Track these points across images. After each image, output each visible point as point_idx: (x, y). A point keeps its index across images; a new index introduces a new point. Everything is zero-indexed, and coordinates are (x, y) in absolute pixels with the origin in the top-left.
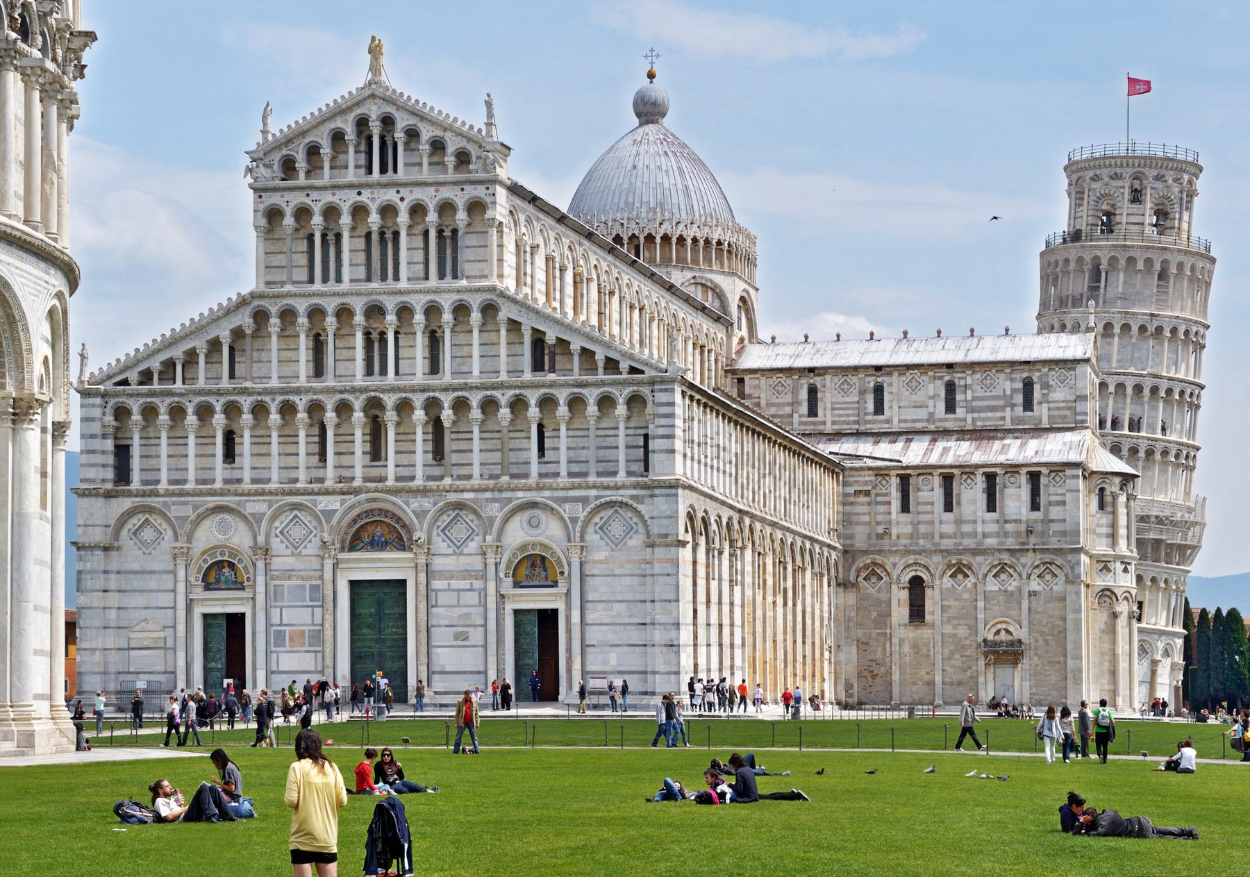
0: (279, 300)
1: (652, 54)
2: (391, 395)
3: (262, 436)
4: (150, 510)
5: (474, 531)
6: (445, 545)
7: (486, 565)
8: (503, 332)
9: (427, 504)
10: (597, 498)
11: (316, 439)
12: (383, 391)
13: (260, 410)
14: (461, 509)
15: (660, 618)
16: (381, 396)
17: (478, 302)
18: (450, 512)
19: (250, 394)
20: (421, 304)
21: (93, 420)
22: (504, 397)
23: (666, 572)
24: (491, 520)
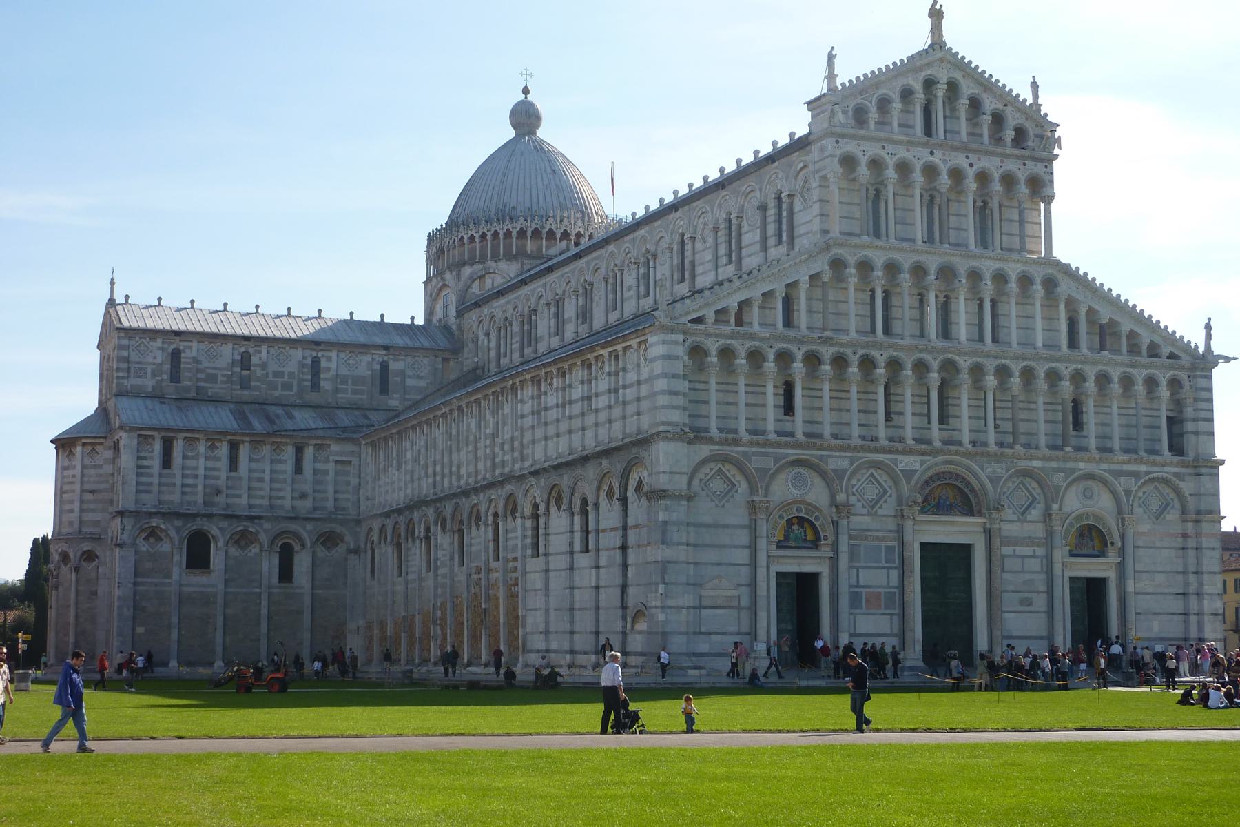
1: (526, 73)
2: (966, 358)
4: (726, 459)
5: (1034, 499)
7: (1050, 534)
8: (1062, 307)
9: (999, 470)
10: (1147, 473)
11: (893, 398)
12: (960, 354)
13: (840, 362)
15: (1207, 589)
17: (1042, 274)
18: (1015, 479)
19: (831, 345)
21: (676, 358)
22: (1066, 370)
23: (1212, 546)
24: (1058, 489)
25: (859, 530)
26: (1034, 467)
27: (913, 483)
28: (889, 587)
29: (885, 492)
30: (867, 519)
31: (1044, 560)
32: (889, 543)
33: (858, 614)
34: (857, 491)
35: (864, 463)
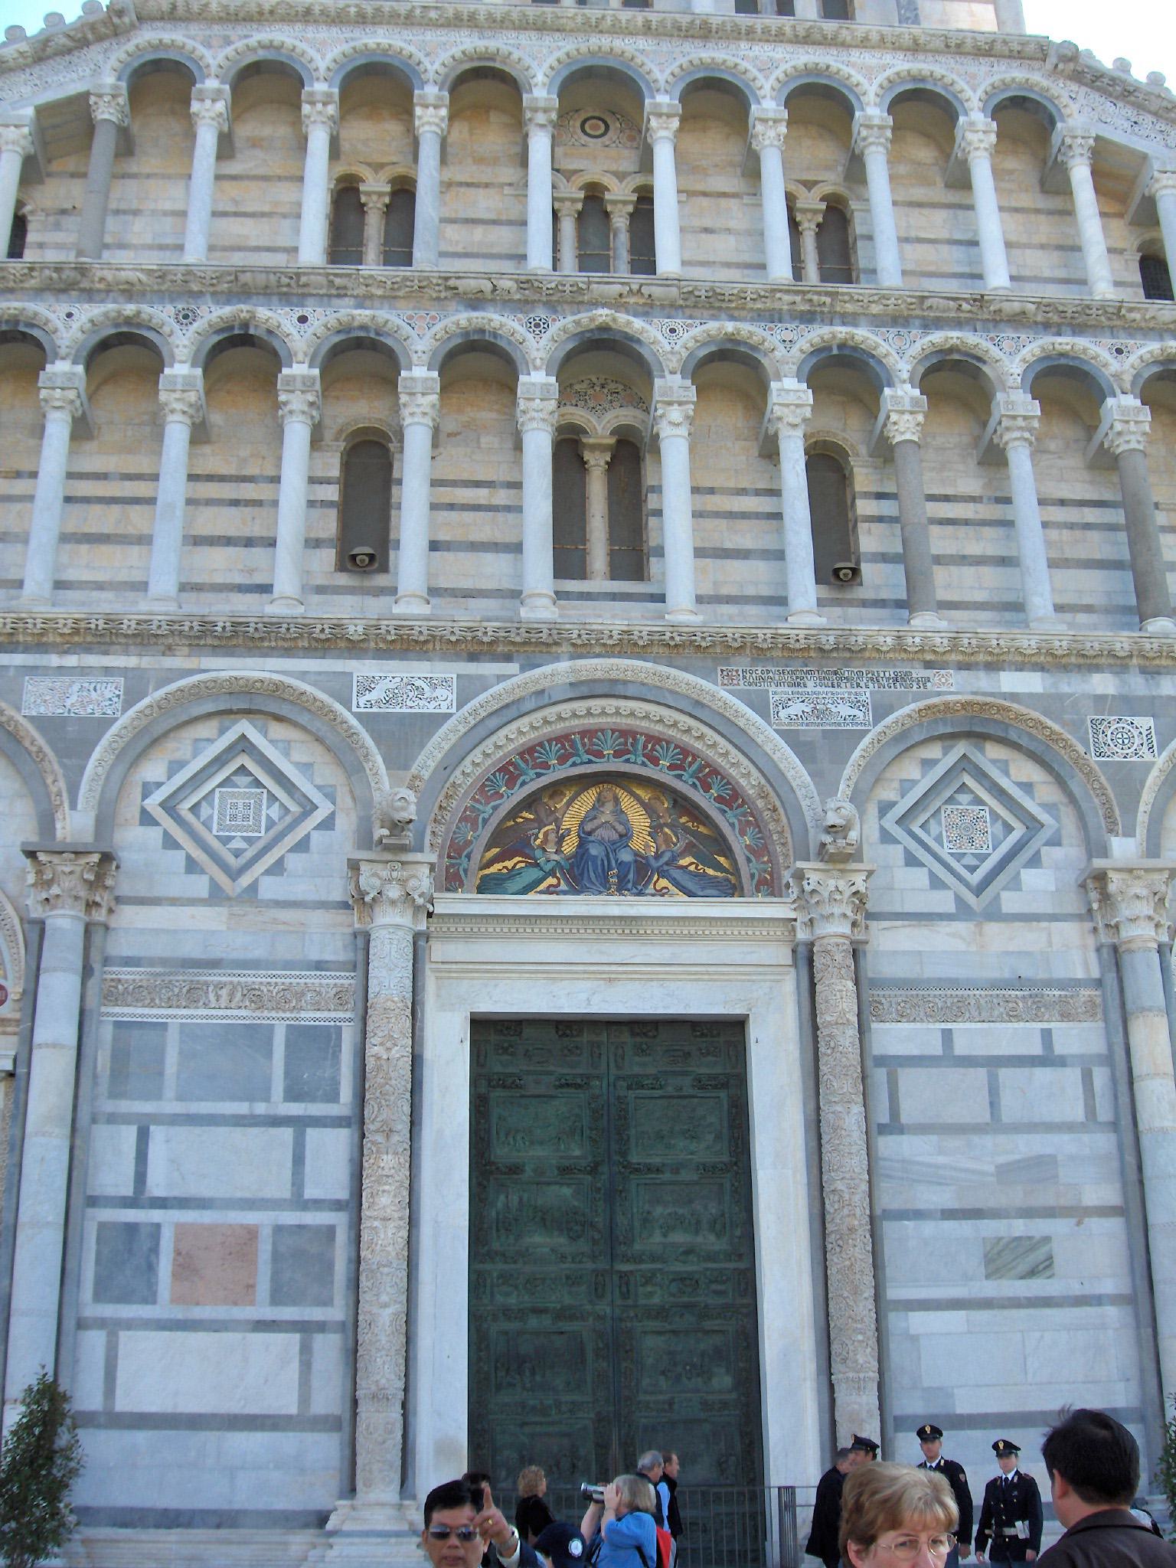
0: (241, 30)
2: (677, 323)
3: (103, 476)
5: (1033, 825)
6: (920, 877)
7: (1115, 957)
8: (1081, 175)
9: (845, 710)
12: (649, 308)
14: (980, 737)
16: (638, 324)
17: (985, 86)
18: (934, 751)
19: (89, 295)
20: (779, 73)
24: (1129, 779)
25: (164, 962)
26: (1014, 697)
27: (429, 757)
28: (301, 1203)
29: (309, 808)
30: (210, 919)
31: (1100, 1077)
32: (309, 1017)
33: (130, 1325)
34: (169, 806)
35: (196, 693)
